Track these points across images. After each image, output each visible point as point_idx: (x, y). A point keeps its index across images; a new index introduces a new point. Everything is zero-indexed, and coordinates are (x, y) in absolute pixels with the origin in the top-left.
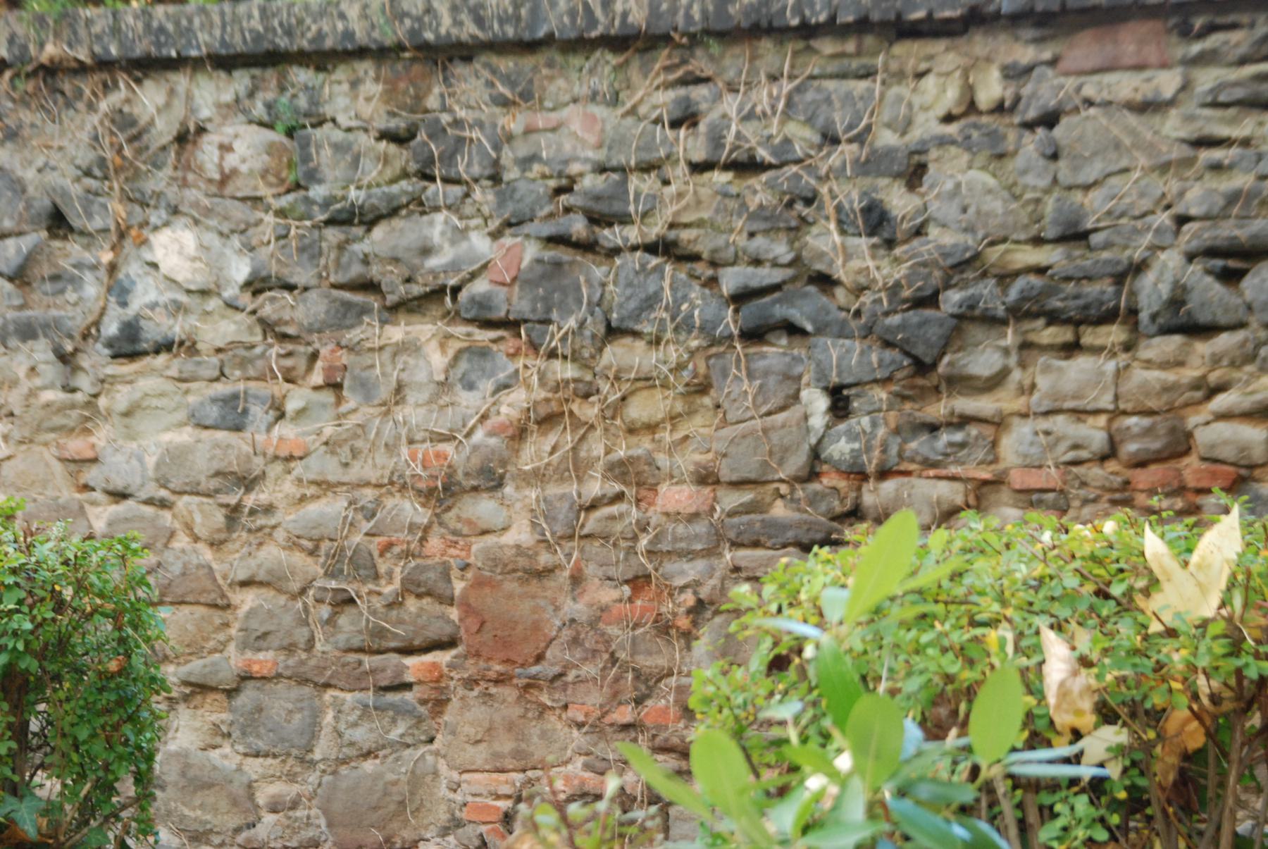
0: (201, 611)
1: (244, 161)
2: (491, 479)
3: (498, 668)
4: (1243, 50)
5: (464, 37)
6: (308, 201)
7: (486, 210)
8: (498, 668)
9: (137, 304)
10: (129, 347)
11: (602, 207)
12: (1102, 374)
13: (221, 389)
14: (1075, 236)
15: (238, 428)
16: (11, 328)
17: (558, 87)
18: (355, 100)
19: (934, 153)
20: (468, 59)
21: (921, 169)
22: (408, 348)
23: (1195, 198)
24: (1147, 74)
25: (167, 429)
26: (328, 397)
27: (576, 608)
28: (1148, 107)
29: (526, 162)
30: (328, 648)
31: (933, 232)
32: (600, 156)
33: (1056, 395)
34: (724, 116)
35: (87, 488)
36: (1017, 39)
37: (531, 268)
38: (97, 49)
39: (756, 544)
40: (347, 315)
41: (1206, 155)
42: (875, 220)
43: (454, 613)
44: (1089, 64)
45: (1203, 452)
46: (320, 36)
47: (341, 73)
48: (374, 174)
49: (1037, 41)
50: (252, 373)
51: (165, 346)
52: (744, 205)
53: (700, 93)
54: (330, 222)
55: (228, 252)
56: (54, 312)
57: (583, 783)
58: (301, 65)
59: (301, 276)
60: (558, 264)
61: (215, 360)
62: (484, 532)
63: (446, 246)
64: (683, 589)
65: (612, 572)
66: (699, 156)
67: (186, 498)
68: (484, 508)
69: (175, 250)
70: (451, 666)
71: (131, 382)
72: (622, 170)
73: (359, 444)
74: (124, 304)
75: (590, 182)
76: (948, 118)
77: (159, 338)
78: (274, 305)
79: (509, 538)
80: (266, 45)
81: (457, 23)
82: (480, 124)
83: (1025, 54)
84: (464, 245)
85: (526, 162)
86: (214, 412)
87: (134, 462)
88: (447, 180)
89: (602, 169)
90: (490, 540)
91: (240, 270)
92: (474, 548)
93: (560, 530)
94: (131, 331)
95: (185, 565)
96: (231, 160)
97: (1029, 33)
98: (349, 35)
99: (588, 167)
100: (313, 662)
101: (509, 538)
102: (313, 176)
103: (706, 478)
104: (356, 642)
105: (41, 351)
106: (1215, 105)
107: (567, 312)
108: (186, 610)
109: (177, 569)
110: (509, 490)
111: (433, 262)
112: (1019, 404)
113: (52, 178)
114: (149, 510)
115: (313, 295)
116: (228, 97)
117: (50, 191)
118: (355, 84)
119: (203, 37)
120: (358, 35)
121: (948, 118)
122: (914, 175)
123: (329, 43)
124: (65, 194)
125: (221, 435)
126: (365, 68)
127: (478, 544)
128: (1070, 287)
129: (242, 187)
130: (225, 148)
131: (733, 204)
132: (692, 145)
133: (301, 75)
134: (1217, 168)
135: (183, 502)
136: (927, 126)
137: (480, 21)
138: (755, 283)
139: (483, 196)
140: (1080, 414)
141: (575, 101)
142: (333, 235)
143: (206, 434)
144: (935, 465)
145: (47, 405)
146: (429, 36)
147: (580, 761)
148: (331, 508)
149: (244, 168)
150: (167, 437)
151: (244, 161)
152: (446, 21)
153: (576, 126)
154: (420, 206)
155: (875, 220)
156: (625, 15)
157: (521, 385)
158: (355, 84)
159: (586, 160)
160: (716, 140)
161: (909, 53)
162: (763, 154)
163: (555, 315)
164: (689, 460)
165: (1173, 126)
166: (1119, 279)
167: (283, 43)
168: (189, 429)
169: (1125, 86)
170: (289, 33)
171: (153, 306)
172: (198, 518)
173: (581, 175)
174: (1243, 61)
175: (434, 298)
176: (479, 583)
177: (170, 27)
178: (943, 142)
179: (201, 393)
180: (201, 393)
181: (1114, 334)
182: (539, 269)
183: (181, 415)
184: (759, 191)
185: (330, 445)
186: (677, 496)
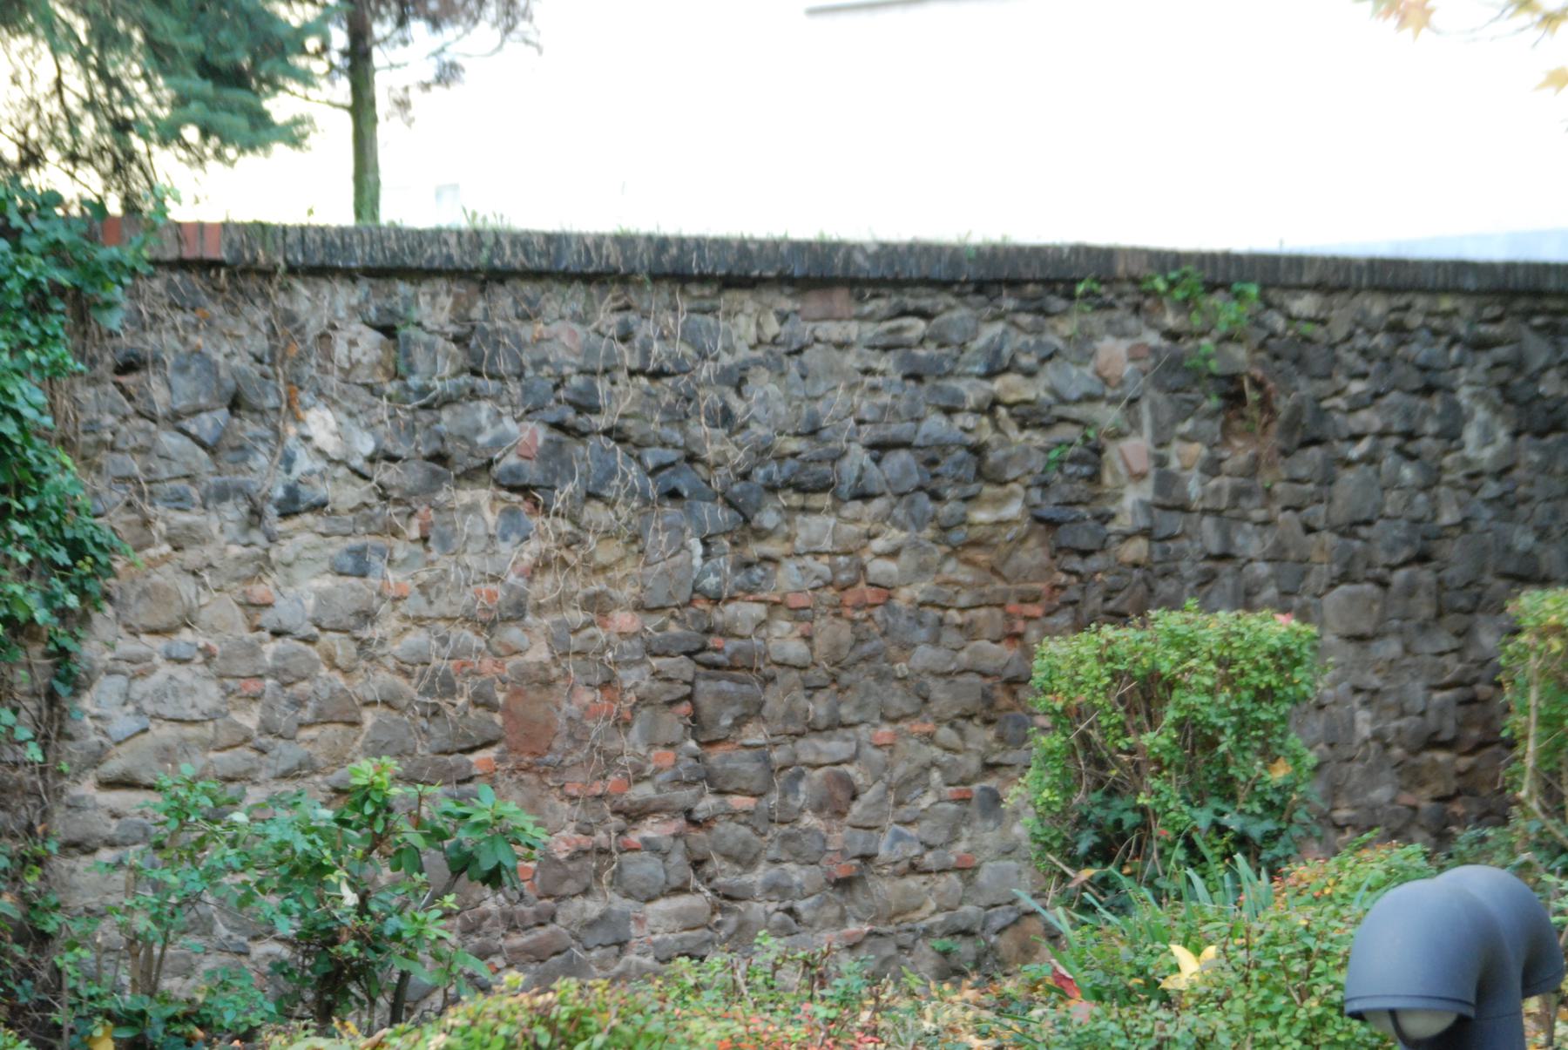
0: (340, 727)
1: (365, 354)
2: (517, 611)
3: (528, 759)
4: (884, 312)
5: (518, 266)
6: (407, 388)
7: (515, 399)
8: (528, 759)
9: (297, 471)
10: (290, 507)
11: (582, 401)
12: (827, 527)
13: (353, 542)
14: (813, 432)
15: (363, 575)
16: (212, 491)
17: (552, 307)
18: (432, 309)
19: (753, 370)
20: (501, 282)
21: (743, 380)
22: (472, 508)
23: (865, 408)
24: (844, 323)
25: (315, 577)
26: (419, 548)
27: (571, 708)
28: (842, 346)
29: (537, 365)
30: (425, 752)
31: (754, 426)
32: (579, 361)
33: (809, 542)
34: (647, 336)
35: (259, 628)
36: (782, 292)
37: (545, 446)
38: (290, 257)
39: (666, 654)
40: (435, 481)
41: (868, 380)
42: (725, 417)
43: (498, 718)
44: (817, 315)
45: (871, 580)
46: (432, 257)
47: (425, 288)
48: (439, 369)
49: (791, 296)
50: (373, 528)
51: (318, 507)
52: (659, 404)
53: (632, 317)
54: (424, 407)
55: (354, 429)
56: (240, 478)
57: (578, 842)
58: (401, 278)
59: (401, 450)
60: (560, 443)
61: (350, 518)
62: (517, 652)
63: (489, 427)
64: (629, 690)
65: (591, 679)
66: (635, 365)
67: (331, 634)
68: (513, 634)
69: (321, 424)
70: (500, 760)
71: (290, 538)
72: (594, 373)
73: (442, 585)
74: (289, 471)
75: (576, 381)
76: (753, 348)
77: (314, 500)
78: (386, 474)
79: (530, 657)
80: (399, 262)
81: (514, 254)
82: (507, 332)
83: (787, 305)
84: (500, 427)
85: (537, 365)
86: (349, 562)
87: (296, 605)
88: (492, 377)
89: (581, 372)
90: (517, 659)
91: (366, 445)
92: (508, 666)
93: (149, 707)
94: (292, 493)
95: (332, 690)
96: (356, 353)
97: (788, 290)
98: (449, 258)
99: (574, 370)
100: (415, 765)
101: (530, 657)
102: (411, 370)
103: (640, 607)
104: (445, 745)
105: (233, 511)
106: (873, 348)
107: (564, 482)
108: (330, 728)
109: (325, 694)
110: (529, 619)
111: (482, 440)
112: (787, 548)
113: (236, 362)
114: (302, 645)
115: (413, 465)
116: (354, 301)
117: (234, 373)
118: (434, 296)
119: (359, 252)
120: (456, 258)
121: (753, 348)
122: (739, 386)
123: (436, 264)
124: (246, 376)
125: (353, 581)
126: (441, 284)
127: (511, 662)
128: (812, 467)
129: (363, 375)
130: (352, 343)
131: (652, 401)
132: (630, 359)
133: (403, 288)
134: (874, 389)
135: (327, 639)
136: (743, 353)
137: (526, 254)
138: (666, 460)
139: (514, 388)
140: (817, 554)
141: (562, 317)
142: (424, 416)
143: (341, 580)
144: (750, 592)
145: (238, 558)
146: (497, 262)
147: (572, 826)
148: (417, 638)
149: (365, 360)
150: (315, 583)
151: (365, 354)
152: (508, 252)
153: (564, 338)
154: (474, 394)
155: (725, 417)
156: (608, 257)
157: (545, 533)
158: (434, 296)
159: (572, 365)
160: (646, 353)
161: (732, 297)
162: (669, 366)
163: (557, 482)
164: (628, 592)
165: (851, 360)
166: (833, 461)
167: (409, 261)
168: (329, 576)
169: (833, 331)
170: (412, 253)
171: (311, 473)
172: (339, 651)
173: (570, 375)
174: (881, 320)
175: (480, 471)
176: (517, 693)
177: (338, 242)
178: (757, 363)
179: (337, 547)
180: (337, 547)
181: (825, 500)
182: (551, 447)
183: (326, 565)
184: (666, 391)
185: (423, 588)
186: (624, 620)
